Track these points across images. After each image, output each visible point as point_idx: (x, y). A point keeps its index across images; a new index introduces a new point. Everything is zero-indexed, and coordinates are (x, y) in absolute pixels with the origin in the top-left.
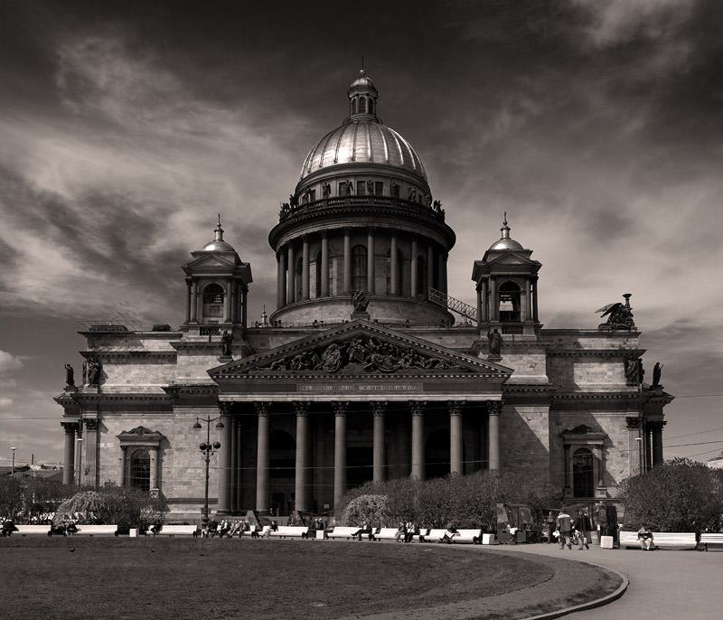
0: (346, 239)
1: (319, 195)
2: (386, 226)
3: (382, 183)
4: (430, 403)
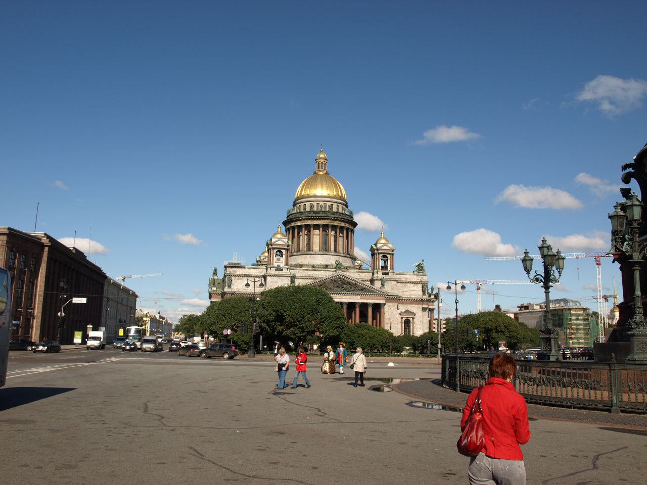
0: (321, 229)
1: (308, 209)
2: (336, 224)
4: (362, 303)
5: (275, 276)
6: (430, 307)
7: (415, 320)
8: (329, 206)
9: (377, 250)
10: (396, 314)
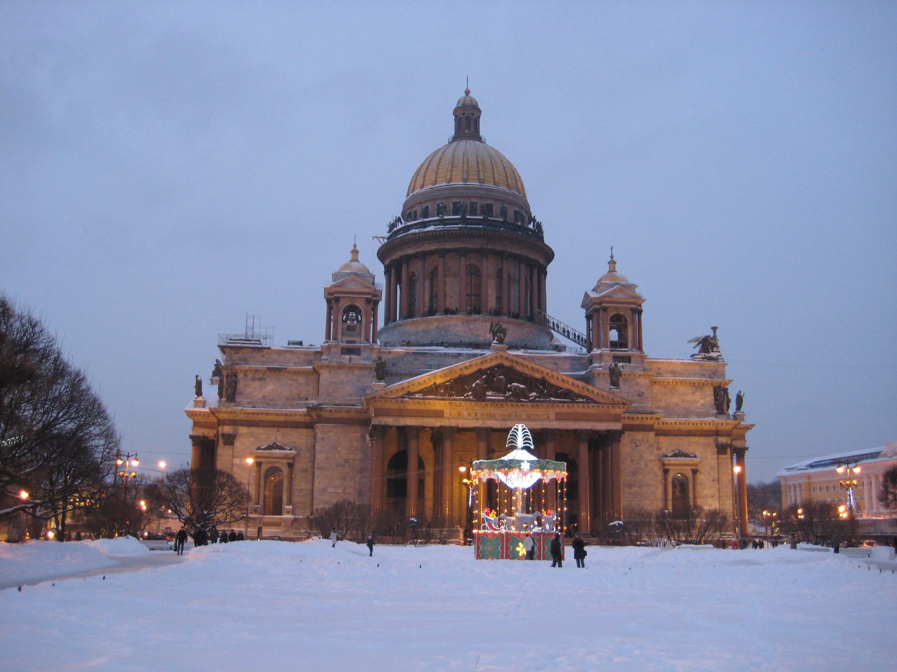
2: (499, 248)
3: (492, 205)
5: (341, 367)
6: (738, 444)
7: (700, 477)
8: (482, 207)
9: (600, 301)
10: (652, 461)
